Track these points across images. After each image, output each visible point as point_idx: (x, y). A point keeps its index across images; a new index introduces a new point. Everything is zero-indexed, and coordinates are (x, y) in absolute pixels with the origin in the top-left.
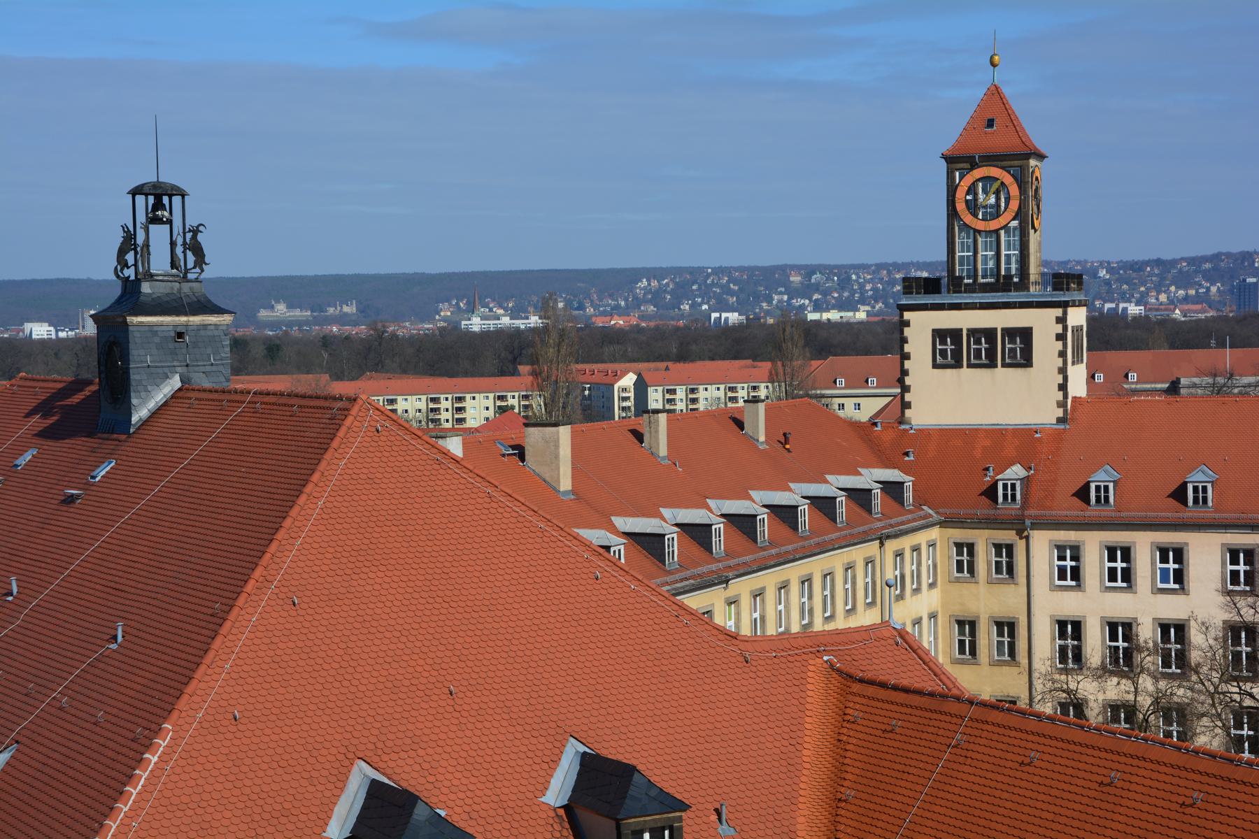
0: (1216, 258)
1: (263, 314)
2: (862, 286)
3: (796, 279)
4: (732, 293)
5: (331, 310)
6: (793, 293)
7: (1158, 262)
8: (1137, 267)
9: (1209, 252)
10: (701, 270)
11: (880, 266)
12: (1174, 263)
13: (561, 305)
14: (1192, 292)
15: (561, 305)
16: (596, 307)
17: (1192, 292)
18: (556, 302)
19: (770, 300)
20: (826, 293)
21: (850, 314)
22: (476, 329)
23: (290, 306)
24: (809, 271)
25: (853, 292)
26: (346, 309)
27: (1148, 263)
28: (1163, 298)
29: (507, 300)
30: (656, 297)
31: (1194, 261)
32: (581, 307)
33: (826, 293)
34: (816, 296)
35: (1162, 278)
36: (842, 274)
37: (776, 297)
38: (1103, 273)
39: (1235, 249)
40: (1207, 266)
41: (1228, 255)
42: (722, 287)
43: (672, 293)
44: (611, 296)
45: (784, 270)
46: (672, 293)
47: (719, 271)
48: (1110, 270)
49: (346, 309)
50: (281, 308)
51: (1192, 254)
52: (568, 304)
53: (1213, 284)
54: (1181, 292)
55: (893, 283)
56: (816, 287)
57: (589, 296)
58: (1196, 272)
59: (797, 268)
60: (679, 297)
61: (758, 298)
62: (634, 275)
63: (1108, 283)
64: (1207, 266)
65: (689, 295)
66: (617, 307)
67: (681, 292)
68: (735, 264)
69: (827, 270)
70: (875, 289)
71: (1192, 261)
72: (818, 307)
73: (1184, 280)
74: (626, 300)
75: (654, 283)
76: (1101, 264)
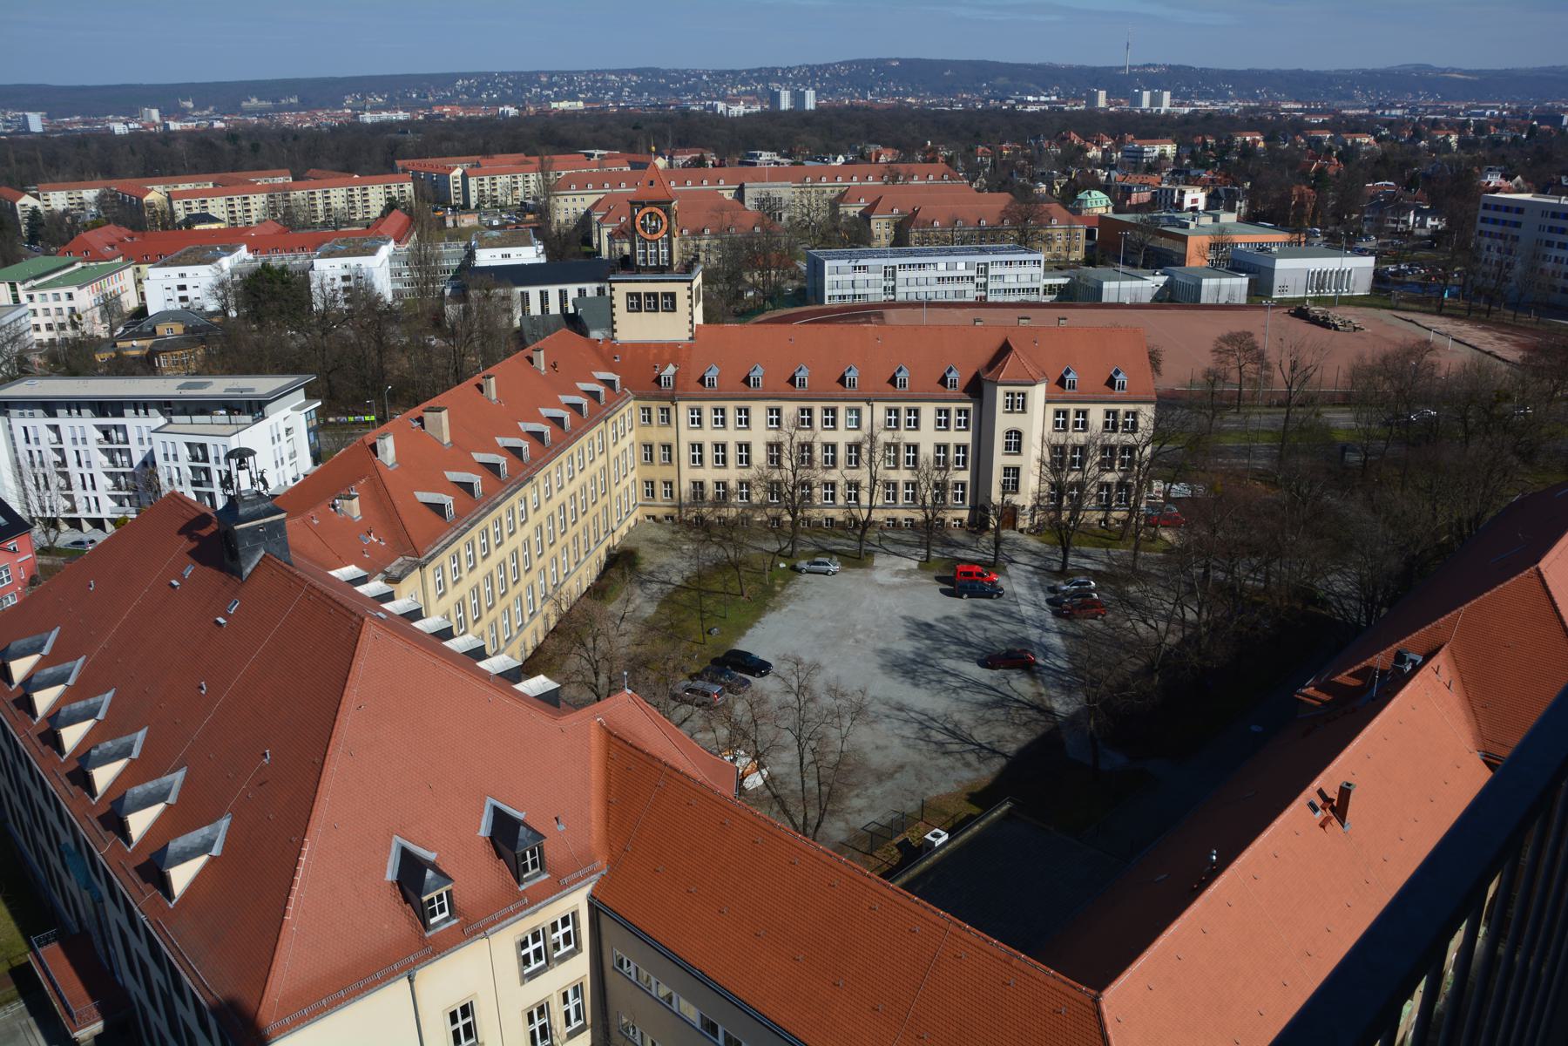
0: (760, 70)
1: (245, 104)
2: (580, 83)
3: (544, 79)
4: (509, 88)
5: (283, 101)
6: (543, 87)
7: (732, 72)
8: (721, 74)
9: (756, 67)
10: (492, 74)
11: (589, 72)
12: (740, 72)
13: (414, 96)
14: (749, 88)
15: (414, 96)
16: (434, 96)
17: (749, 88)
18: (411, 94)
19: (530, 92)
20: (561, 87)
21: (574, 103)
22: (369, 120)
23: (260, 100)
24: (551, 74)
25: (575, 87)
26: (292, 100)
27: (727, 72)
28: (735, 91)
29: (384, 93)
30: (467, 90)
31: (749, 72)
32: (426, 97)
33: (561, 87)
34: (555, 89)
35: (734, 79)
36: (569, 76)
37: (534, 90)
38: (705, 77)
39: (769, 66)
40: (756, 74)
41: (766, 69)
42: (503, 84)
43: (476, 87)
44: (442, 89)
45: (538, 73)
46: (476, 87)
47: (502, 74)
48: (709, 76)
49: (292, 100)
50: (254, 101)
51: (747, 68)
52: (419, 96)
53: (759, 84)
54: (743, 88)
55: (596, 81)
56: (555, 84)
57: (429, 90)
58: (751, 77)
59: (545, 73)
60: (480, 90)
61: (524, 90)
62: (454, 77)
63: (707, 83)
64: (756, 74)
65: (486, 89)
66: (446, 96)
67: (481, 87)
68: (511, 70)
69: (561, 74)
70: (586, 85)
71: (749, 71)
72: (558, 99)
73: (744, 82)
74: (451, 92)
75: (466, 82)
76: (704, 73)
